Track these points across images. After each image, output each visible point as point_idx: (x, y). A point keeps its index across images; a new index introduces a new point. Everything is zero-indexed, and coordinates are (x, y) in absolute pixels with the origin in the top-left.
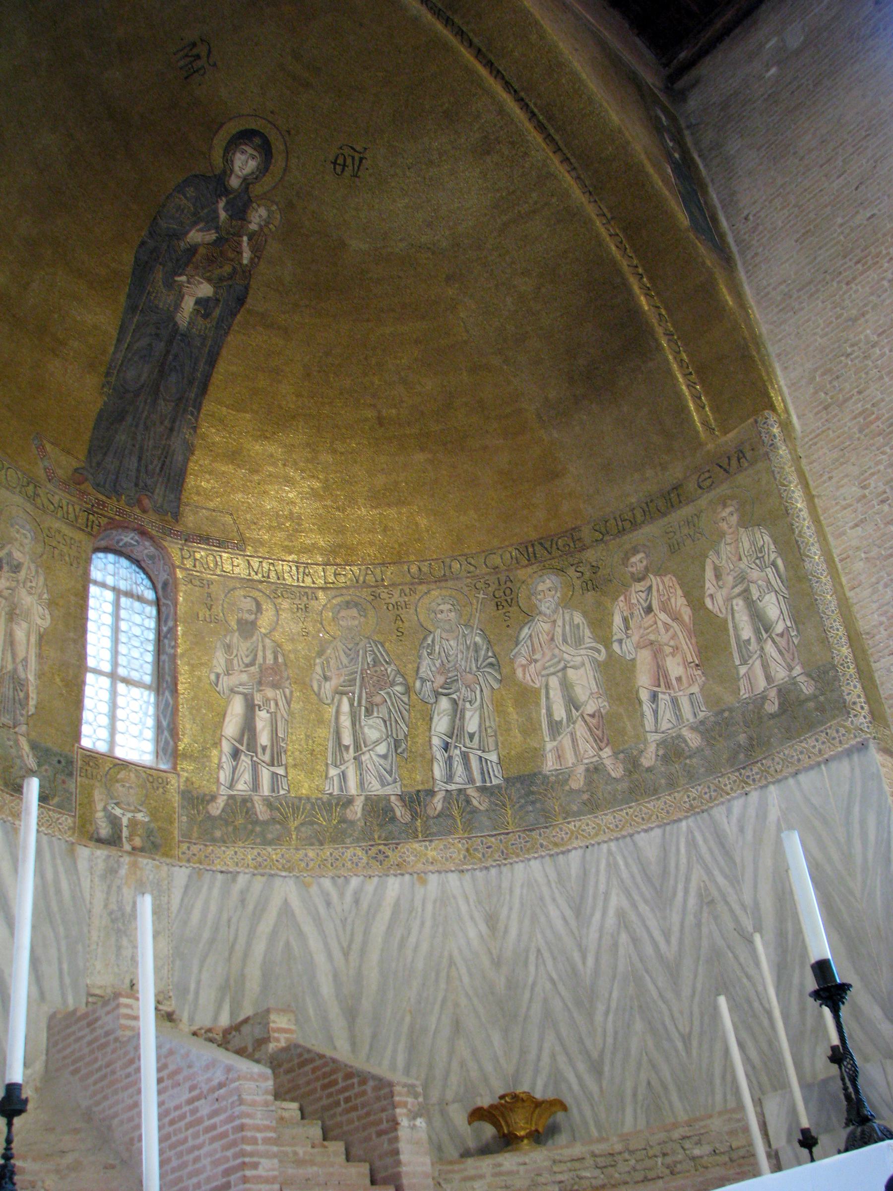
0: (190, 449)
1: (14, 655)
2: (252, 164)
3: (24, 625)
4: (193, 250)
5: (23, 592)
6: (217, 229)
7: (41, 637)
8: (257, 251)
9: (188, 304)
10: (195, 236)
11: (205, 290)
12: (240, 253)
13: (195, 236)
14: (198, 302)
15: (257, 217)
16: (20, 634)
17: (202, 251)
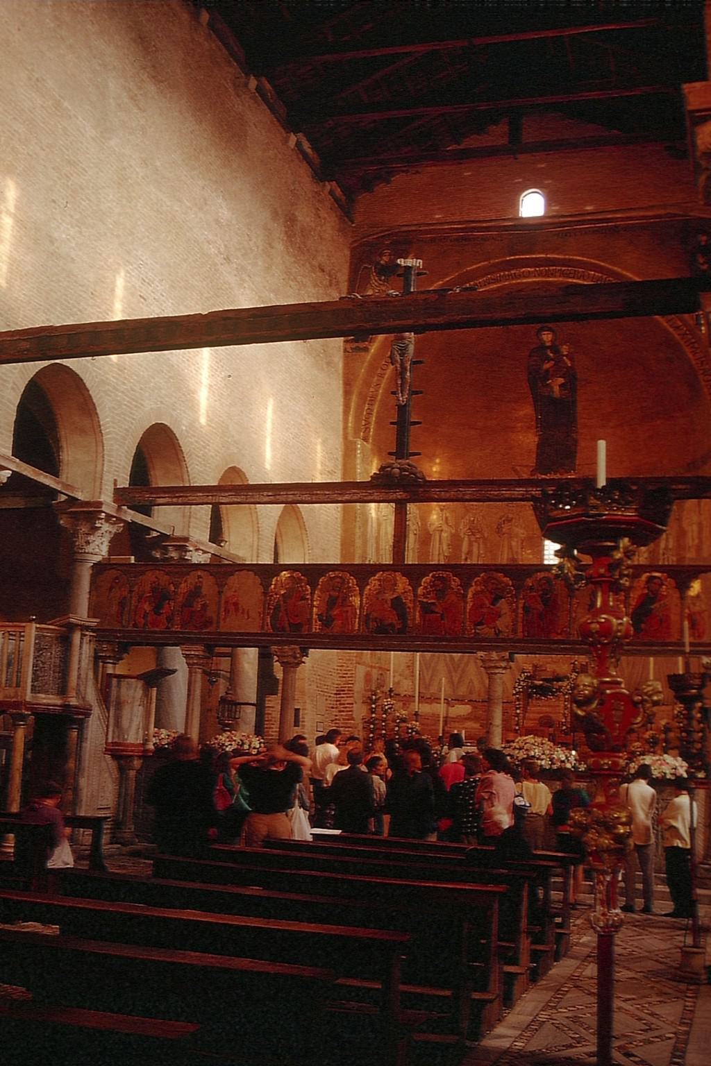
0: (576, 441)
1: (512, 552)
2: (550, 336)
3: (516, 540)
4: (547, 371)
5: (514, 528)
6: (552, 360)
7: (523, 541)
8: (571, 359)
9: (556, 389)
10: (547, 366)
11: (561, 380)
12: (566, 364)
13: (547, 366)
14: (560, 386)
15: (565, 350)
16: (514, 544)
17: (551, 369)
